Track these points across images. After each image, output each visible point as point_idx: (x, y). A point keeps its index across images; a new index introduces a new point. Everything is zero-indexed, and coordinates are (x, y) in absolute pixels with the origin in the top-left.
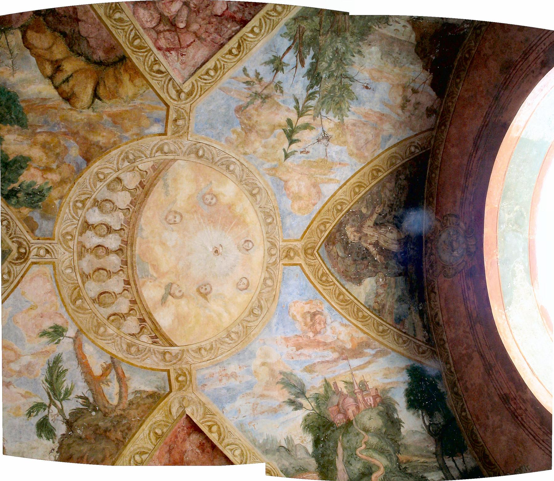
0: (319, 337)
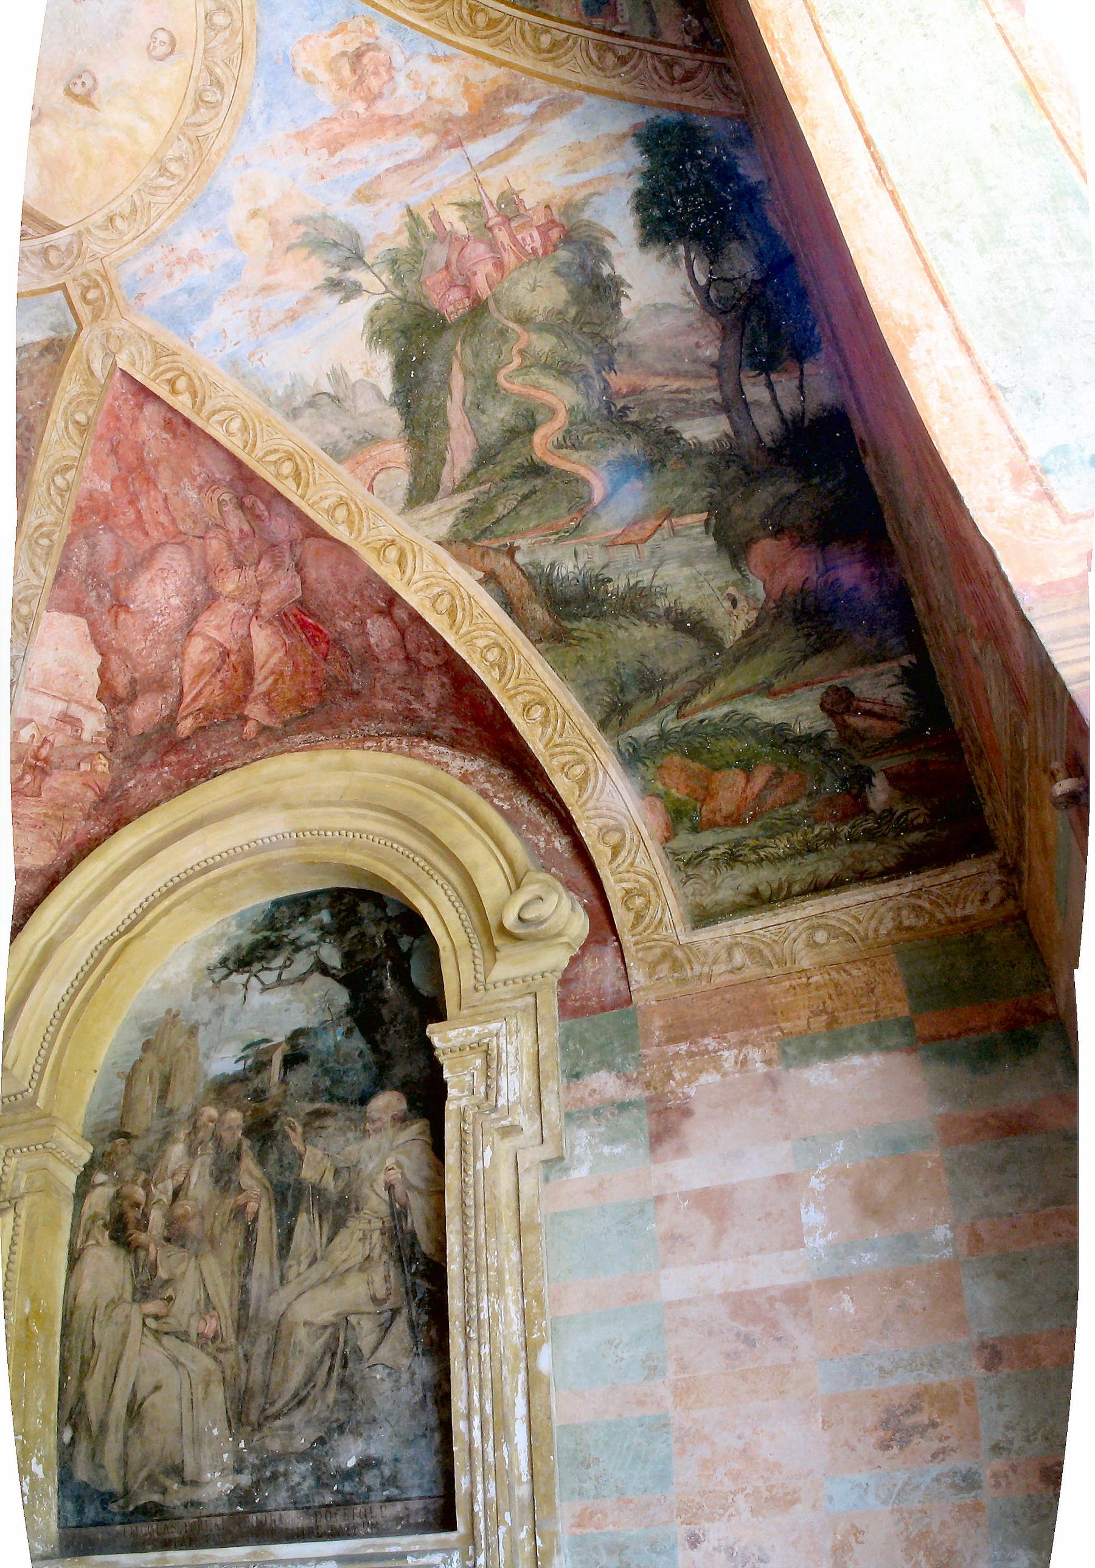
0: (382, 108)
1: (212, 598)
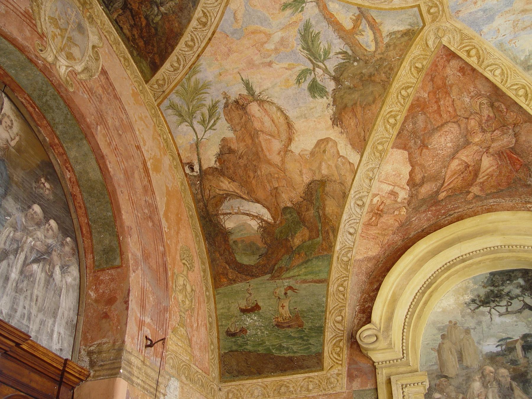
1: (467, 143)
